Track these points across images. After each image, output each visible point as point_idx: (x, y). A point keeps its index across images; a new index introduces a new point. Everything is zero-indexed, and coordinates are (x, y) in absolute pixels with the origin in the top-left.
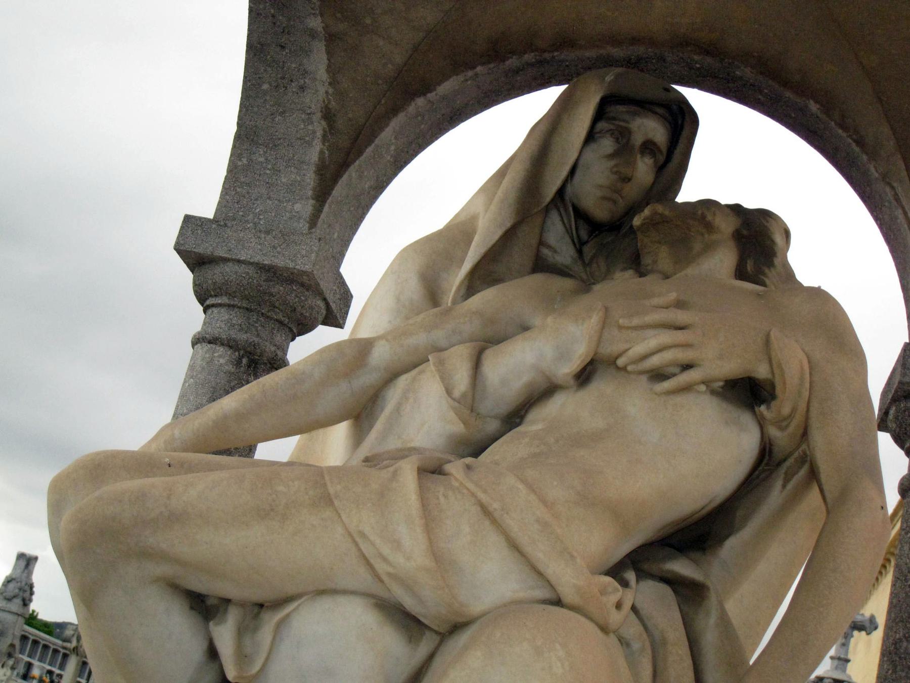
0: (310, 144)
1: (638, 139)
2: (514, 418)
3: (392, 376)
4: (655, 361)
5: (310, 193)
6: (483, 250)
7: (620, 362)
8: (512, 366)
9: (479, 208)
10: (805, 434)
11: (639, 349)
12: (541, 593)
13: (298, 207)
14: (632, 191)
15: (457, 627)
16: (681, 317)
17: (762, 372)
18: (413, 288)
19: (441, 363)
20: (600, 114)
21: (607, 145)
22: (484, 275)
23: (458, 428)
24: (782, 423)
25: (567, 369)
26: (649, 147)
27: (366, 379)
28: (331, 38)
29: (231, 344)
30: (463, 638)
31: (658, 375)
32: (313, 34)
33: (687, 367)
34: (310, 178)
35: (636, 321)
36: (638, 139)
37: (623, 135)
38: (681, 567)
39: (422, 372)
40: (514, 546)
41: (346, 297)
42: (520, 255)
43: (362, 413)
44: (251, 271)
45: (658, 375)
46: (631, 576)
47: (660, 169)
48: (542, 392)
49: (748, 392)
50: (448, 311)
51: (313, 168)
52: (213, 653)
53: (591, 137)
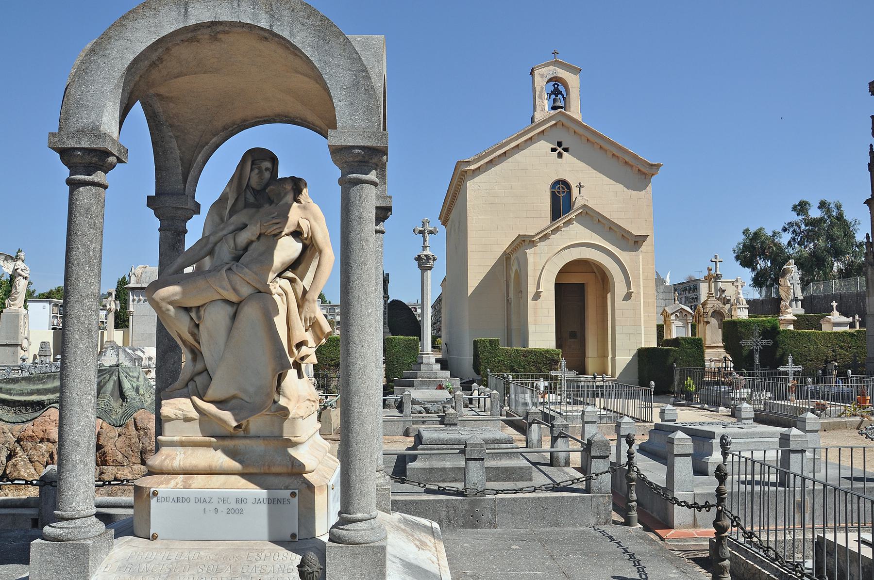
1: (264, 168)
2: (246, 249)
3: (216, 244)
4: (273, 233)
8: (244, 237)
9: (228, 190)
11: (269, 231)
14: (265, 181)
16: (277, 221)
18: (217, 219)
20: (253, 164)
21: (256, 171)
22: (233, 212)
24: (306, 239)
25: (254, 238)
26: (267, 169)
27: (210, 246)
28: (177, 137)
30: (243, 304)
32: (171, 137)
34: (181, 177)
36: (264, 168)
37: (260, 169)
41: (198, 206)
42: (241, 203)
43: (211, 253)
47: (272, 173)
48: (250, 243)
52: (192, 318)
53: (252, 170)
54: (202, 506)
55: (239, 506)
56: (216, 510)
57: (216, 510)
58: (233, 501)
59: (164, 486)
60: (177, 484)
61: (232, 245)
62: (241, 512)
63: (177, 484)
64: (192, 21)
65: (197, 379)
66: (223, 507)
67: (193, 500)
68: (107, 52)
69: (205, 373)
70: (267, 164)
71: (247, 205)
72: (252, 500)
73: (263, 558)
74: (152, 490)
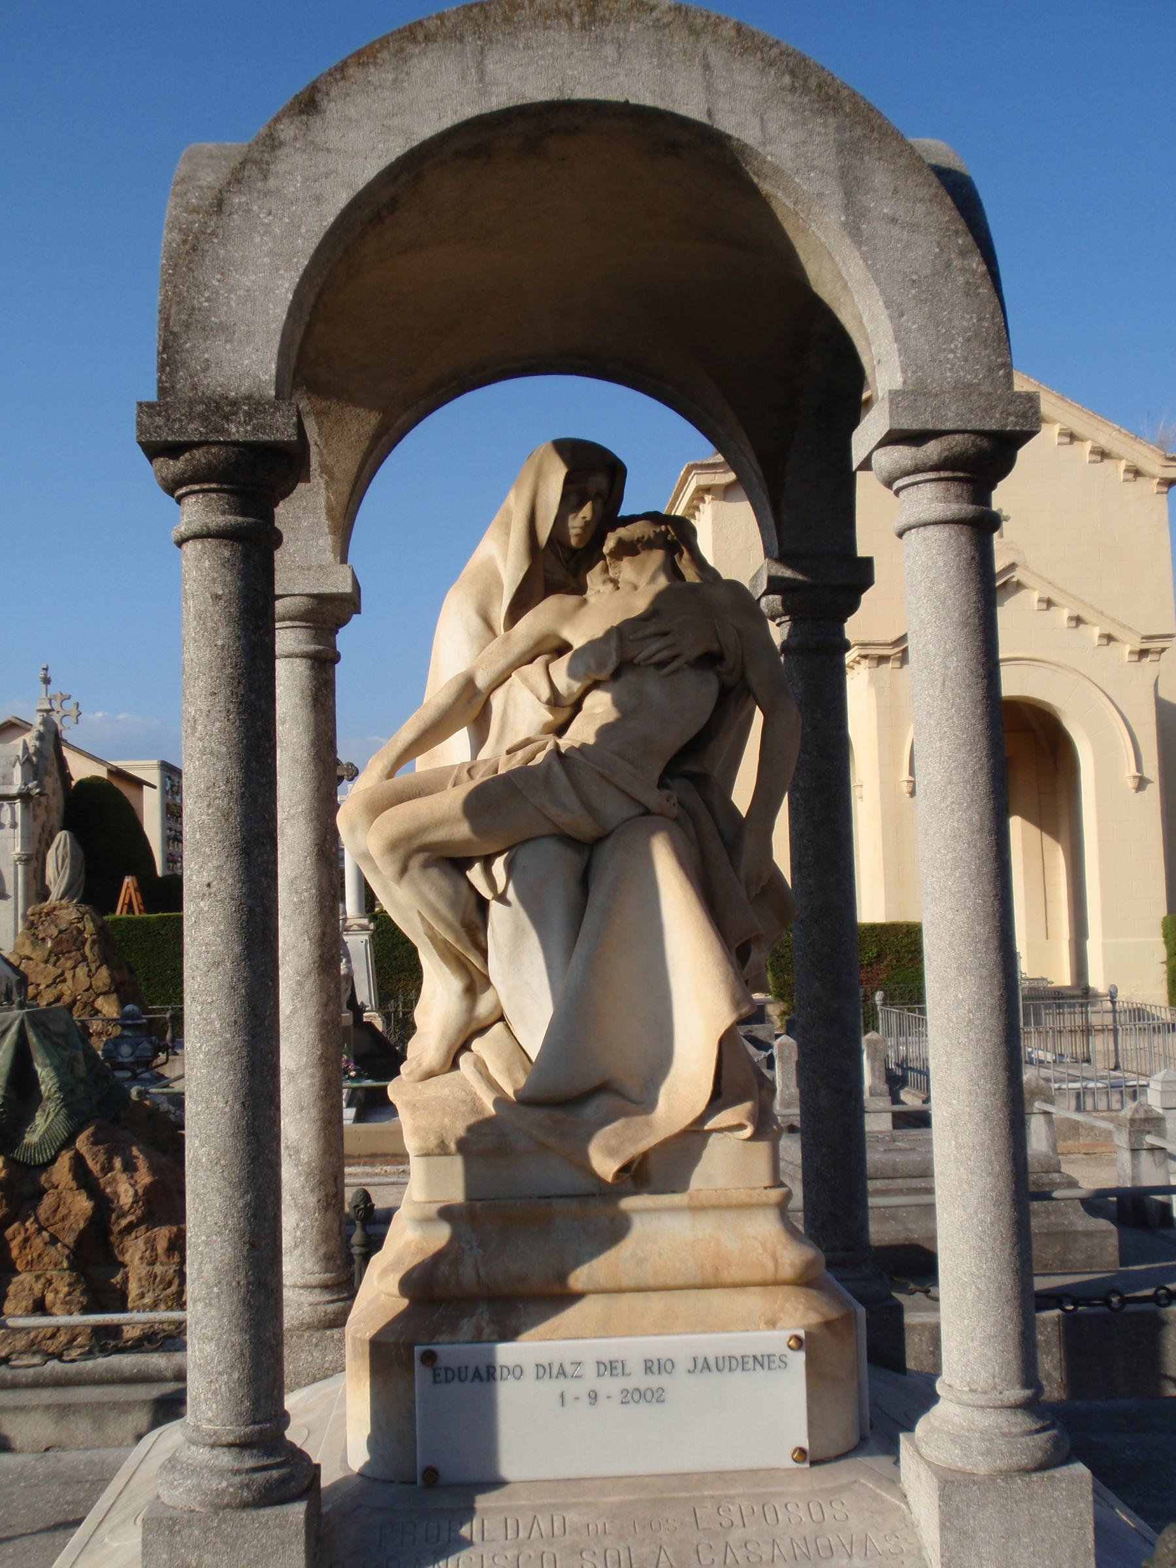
0: (317, 493)
4: (657, 658)
5: (327, 530)
6: (514, 589)
7: (636, 661)
10: (743, 675)
12: (641, 810)
13: (321, 542)
15: (599, 840)
17: (715, 647)
19: (525, 680)
23: (548, 717)
29: (305, 656)
30: (608, 844)
31: (661, 665)
33: (675, 657)
35: (640, 635)
38: (692, 767)
39: (511, 686)
40: (623, 791)
44: (305, 599)
45: (661, 665)
46: (668, 781)
49: (709, 660)
50: (507, 639)
51: (324, 511)
54: (553, 1387)
55: (654, 1381)
56: (593, 1397)
57: (593, 1397)
58: (635, 1366)
59: (444, 1337)
60: (479, 1330)
61: (545, 693)
62: (657, 1396)
63: (479, 1330)
64: (497, 101)
65: (476, 1045)
66: (610, 1386)
67: (530, 1371)
68: (272, 183)
69: (499, 1026)
70: (599, 481)
71: (551, 588)
72: (684, 1363)
73: (738, 1521)
74: (418, 1350)
